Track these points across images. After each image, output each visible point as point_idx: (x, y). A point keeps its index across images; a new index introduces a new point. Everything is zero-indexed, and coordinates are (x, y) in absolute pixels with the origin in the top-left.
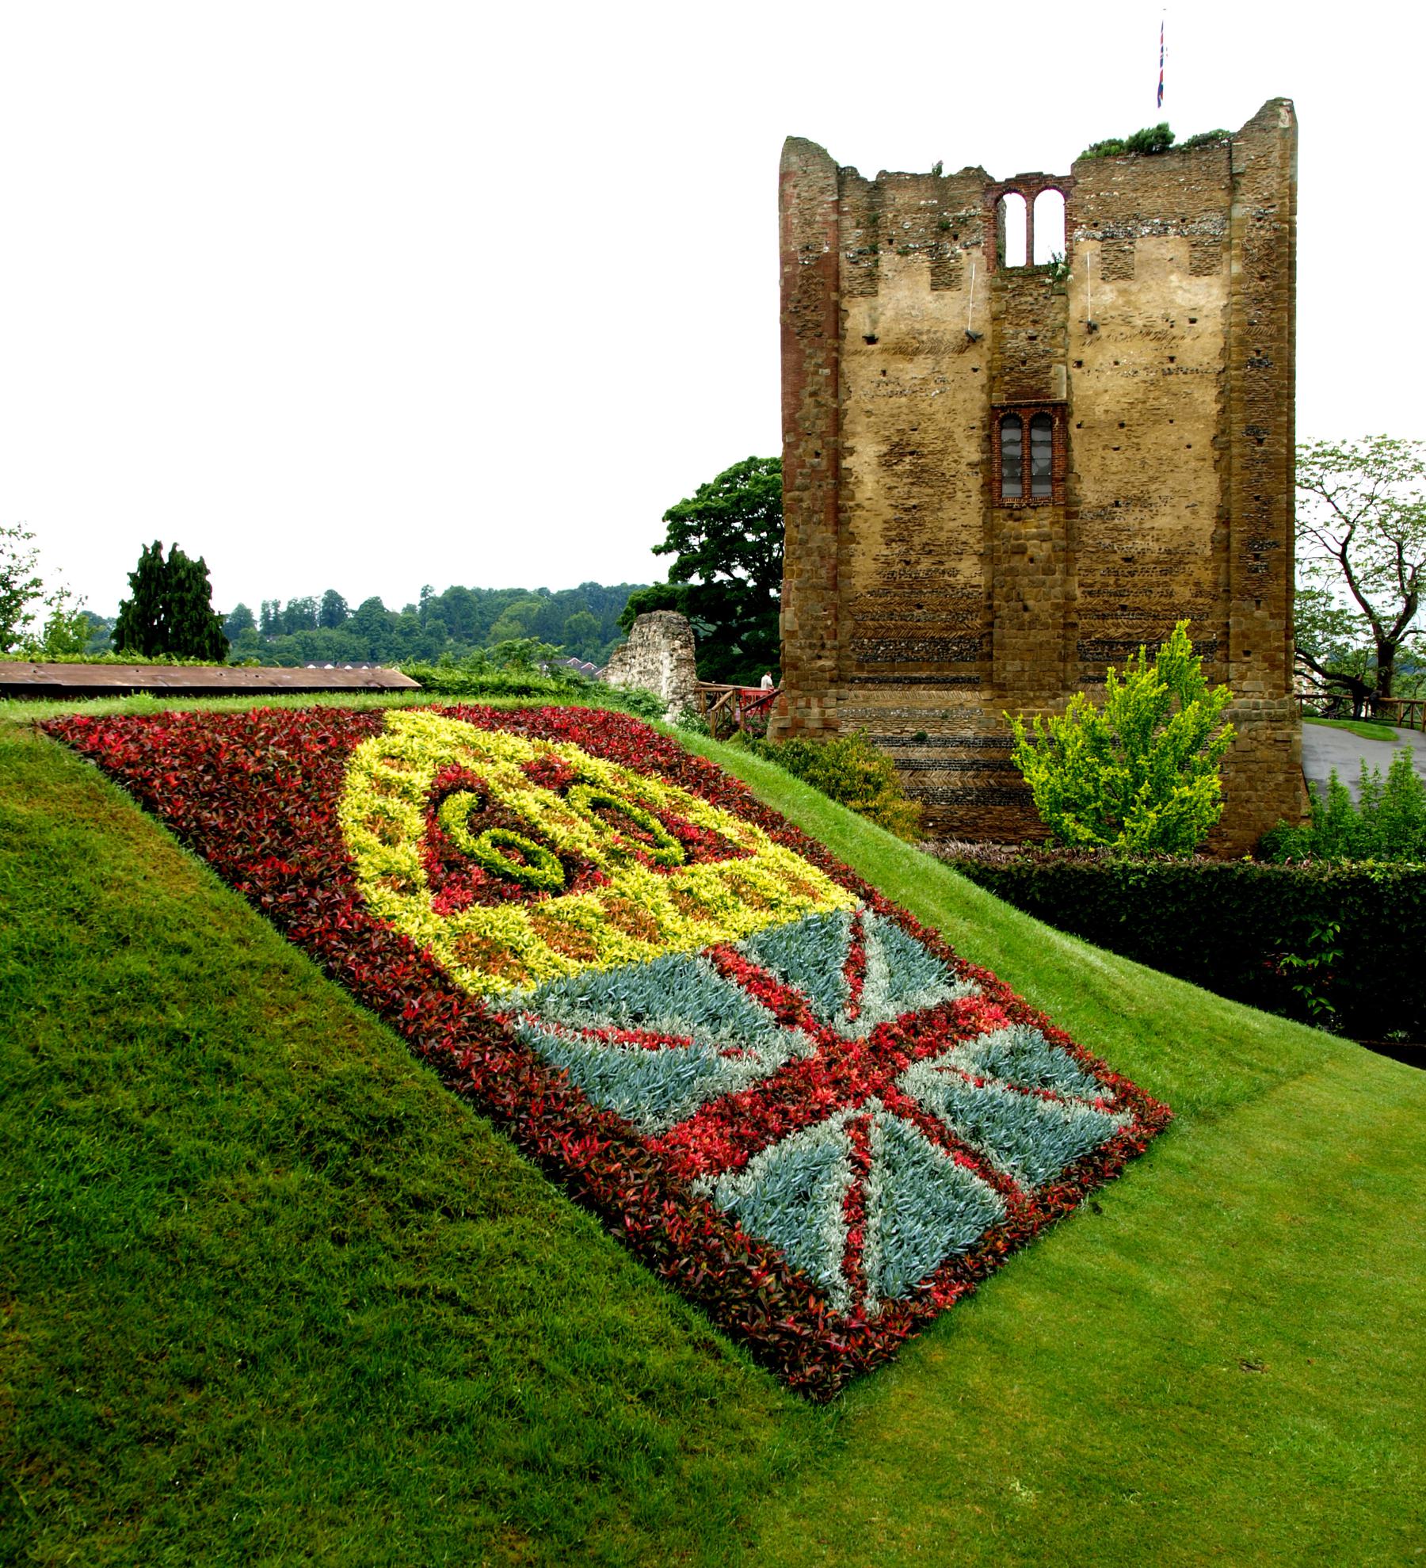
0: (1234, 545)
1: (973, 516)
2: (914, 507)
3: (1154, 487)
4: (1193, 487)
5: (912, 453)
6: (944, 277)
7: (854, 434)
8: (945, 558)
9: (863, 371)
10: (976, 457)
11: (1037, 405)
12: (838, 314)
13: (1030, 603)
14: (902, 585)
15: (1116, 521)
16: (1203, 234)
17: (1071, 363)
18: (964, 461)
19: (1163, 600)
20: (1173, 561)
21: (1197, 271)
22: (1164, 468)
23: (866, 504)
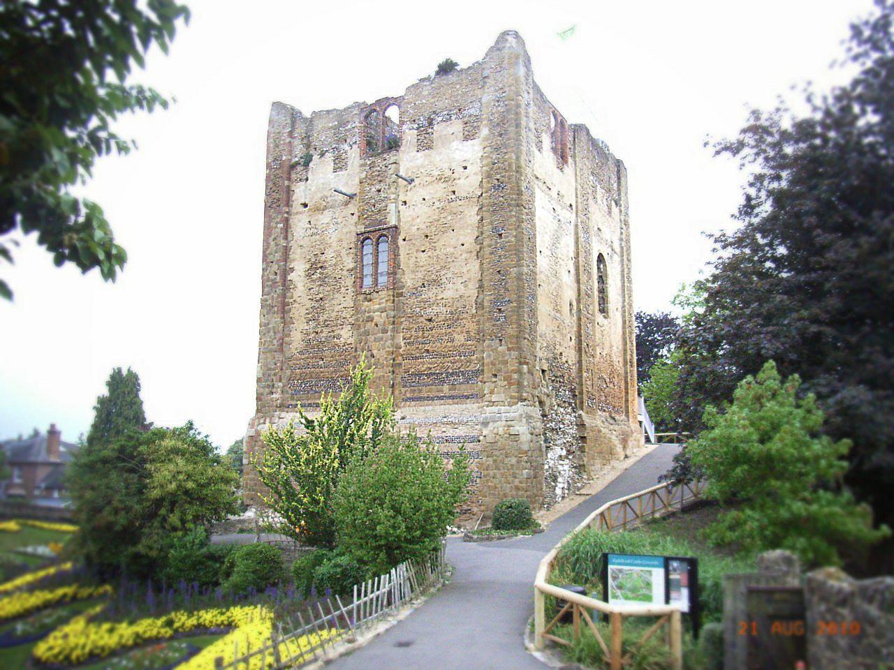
0: (486, 304)
2: (321, 299)
3: (443, 273)
4: (465, 270)
5: (321, 267)
7: (294, 260)
8: (335, 328)
9: (300, 224)
10: (351, 265)
11: (379, 230)
12: (289, 191)
13: (375, 352)
14: (314, 347)
15: (423, 296)
16: (470, 116)
17: (400, 203)
18: (345, 269)
19: (449, 344)
20: (454, 319)
21: (466, 138)
22: (449, 260)
23: (298, 300)
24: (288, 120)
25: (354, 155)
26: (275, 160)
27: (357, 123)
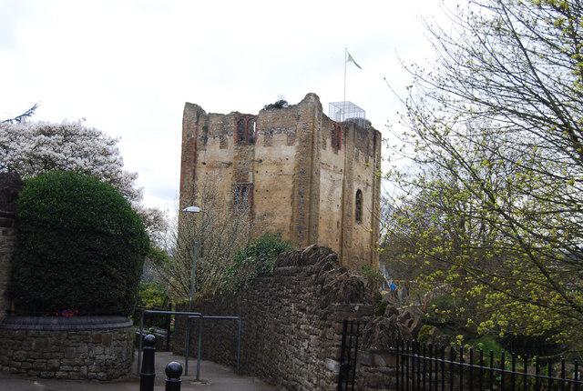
6: (223, 145)
12: (196, 155)
21: (289, 145)
24: (194, 114)
25: (231, 140)
26: (188, 136)
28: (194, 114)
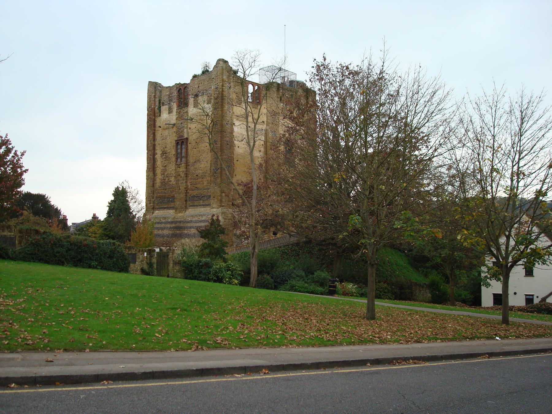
1: (173, 168)
6: (170, 111)
12: (155, 121)
24: (155, 88)
25: (175, 106)
27: (175, 94)
28: (155, 88)
